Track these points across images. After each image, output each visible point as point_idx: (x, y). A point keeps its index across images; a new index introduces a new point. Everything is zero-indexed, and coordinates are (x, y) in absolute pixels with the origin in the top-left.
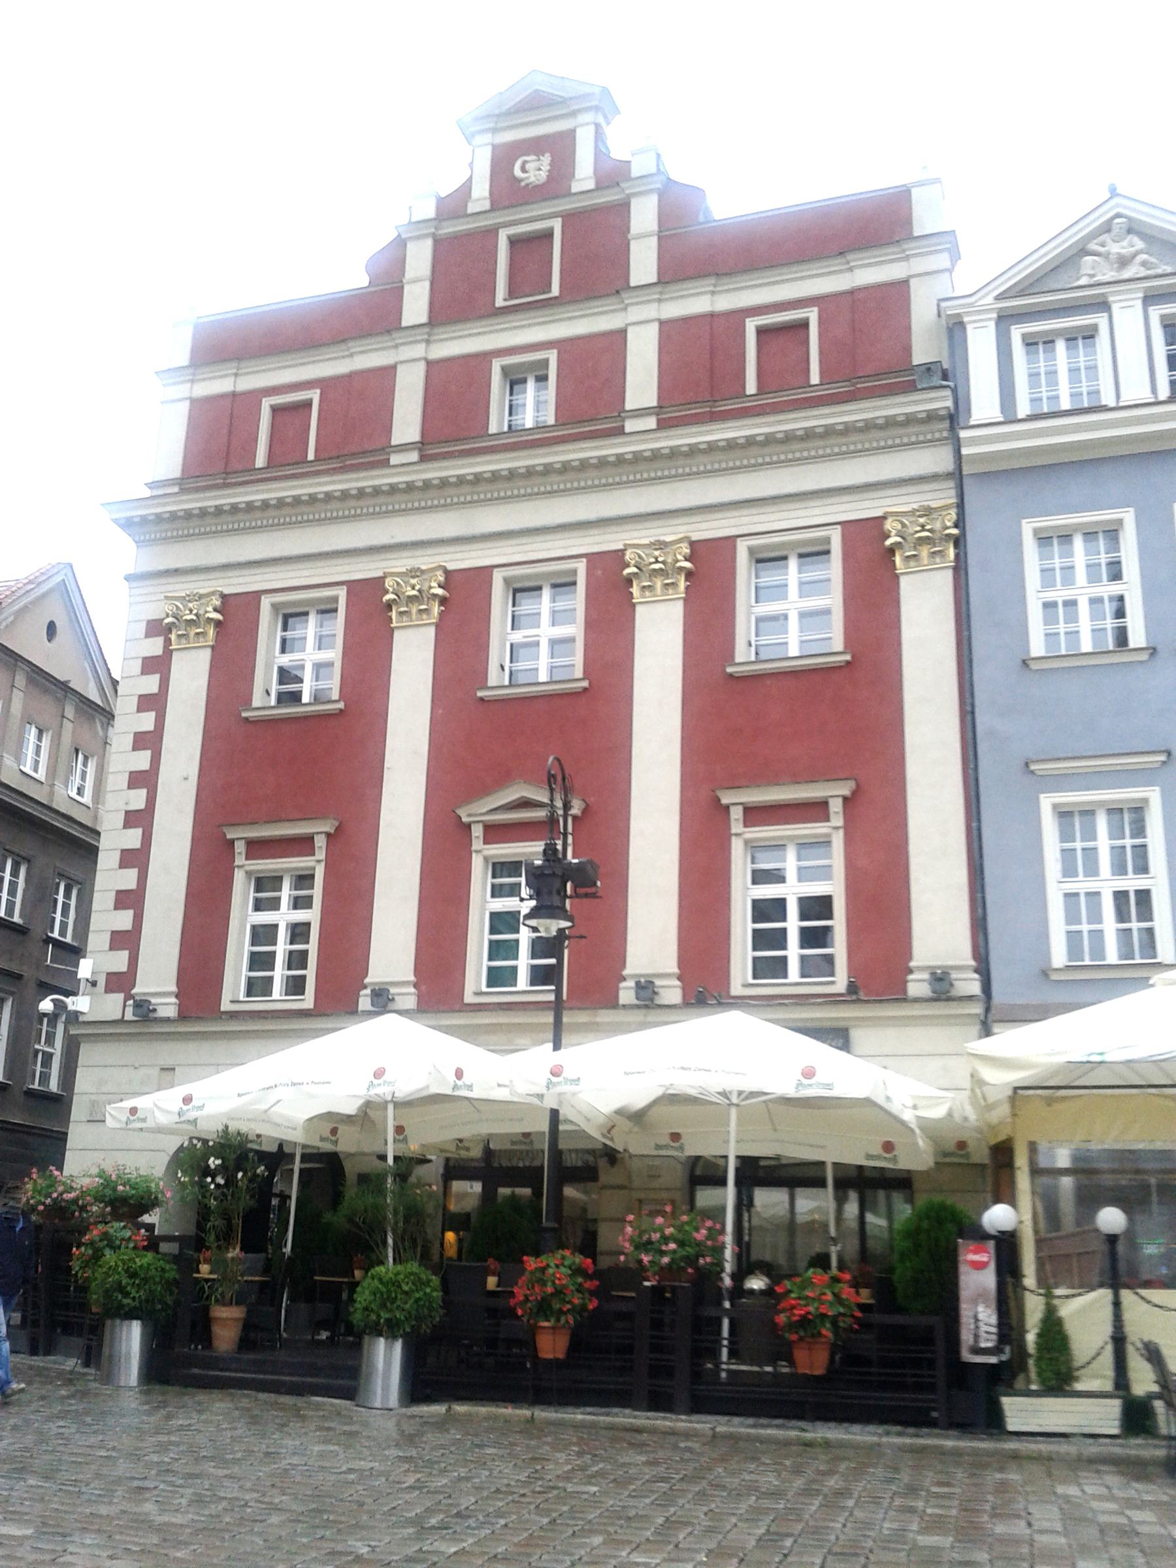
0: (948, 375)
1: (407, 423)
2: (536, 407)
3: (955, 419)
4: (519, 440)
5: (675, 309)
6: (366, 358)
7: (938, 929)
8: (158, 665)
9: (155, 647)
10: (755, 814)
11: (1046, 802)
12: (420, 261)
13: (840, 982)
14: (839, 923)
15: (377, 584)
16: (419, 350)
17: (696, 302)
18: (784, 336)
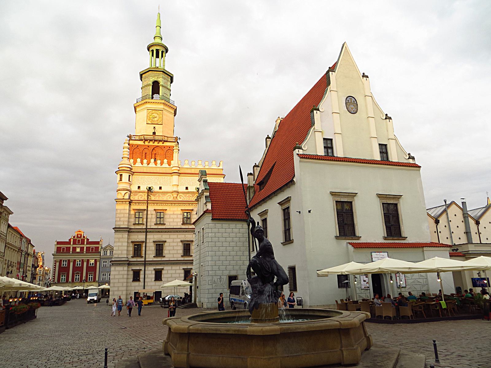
0: (100, 252)
1: (71, 251)
2: (78, 250)
3: (100, 255)
4: (78, 253)
5: (87, 246)
6: (69, 246)
7: (97, 279)
8: (55, 263)
9: (55, 262)
10: (89, 273)
11: (102, 274)
12: (72, 240)
13: (93, 281)
14: (93, 278)
15: (69, 260)
16: (72, 246)
17: (88, 246)
18: (92, 249)
